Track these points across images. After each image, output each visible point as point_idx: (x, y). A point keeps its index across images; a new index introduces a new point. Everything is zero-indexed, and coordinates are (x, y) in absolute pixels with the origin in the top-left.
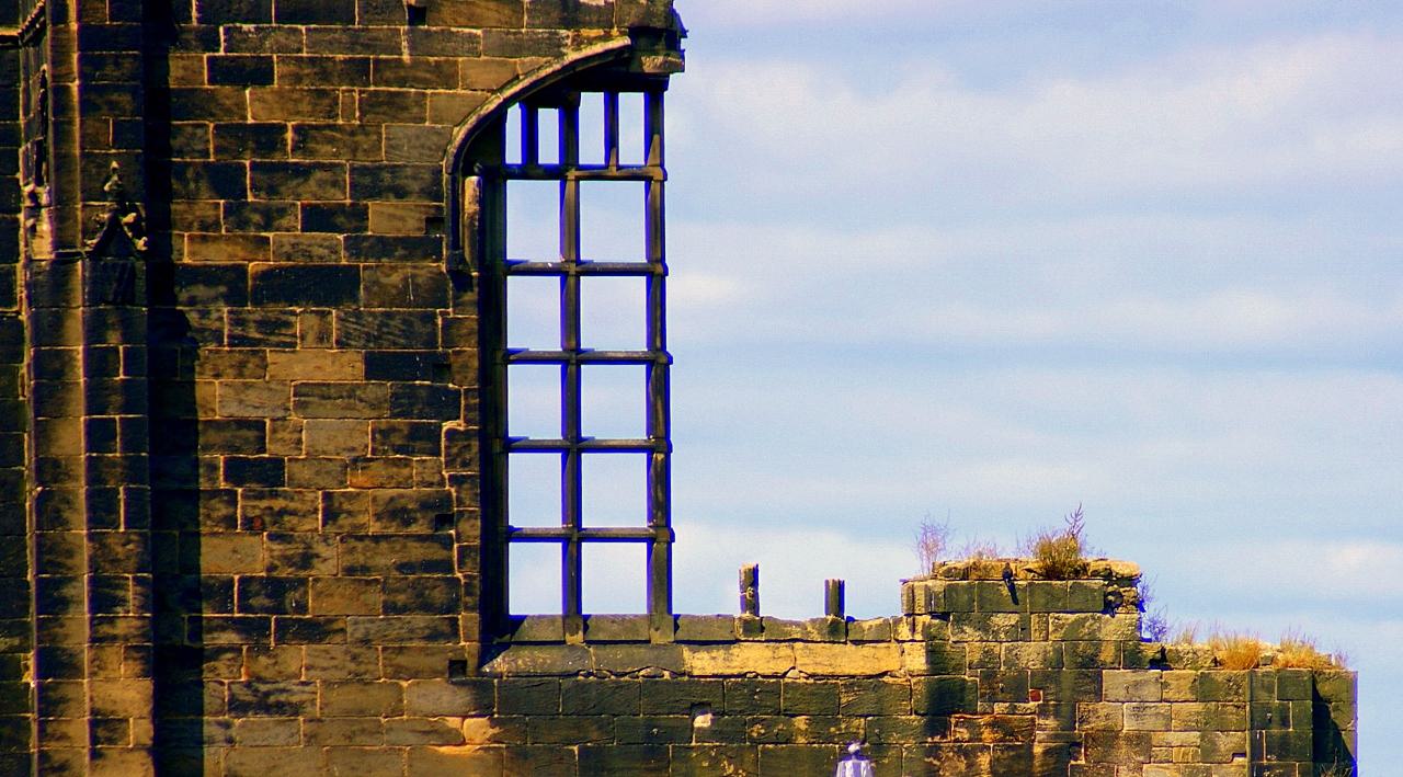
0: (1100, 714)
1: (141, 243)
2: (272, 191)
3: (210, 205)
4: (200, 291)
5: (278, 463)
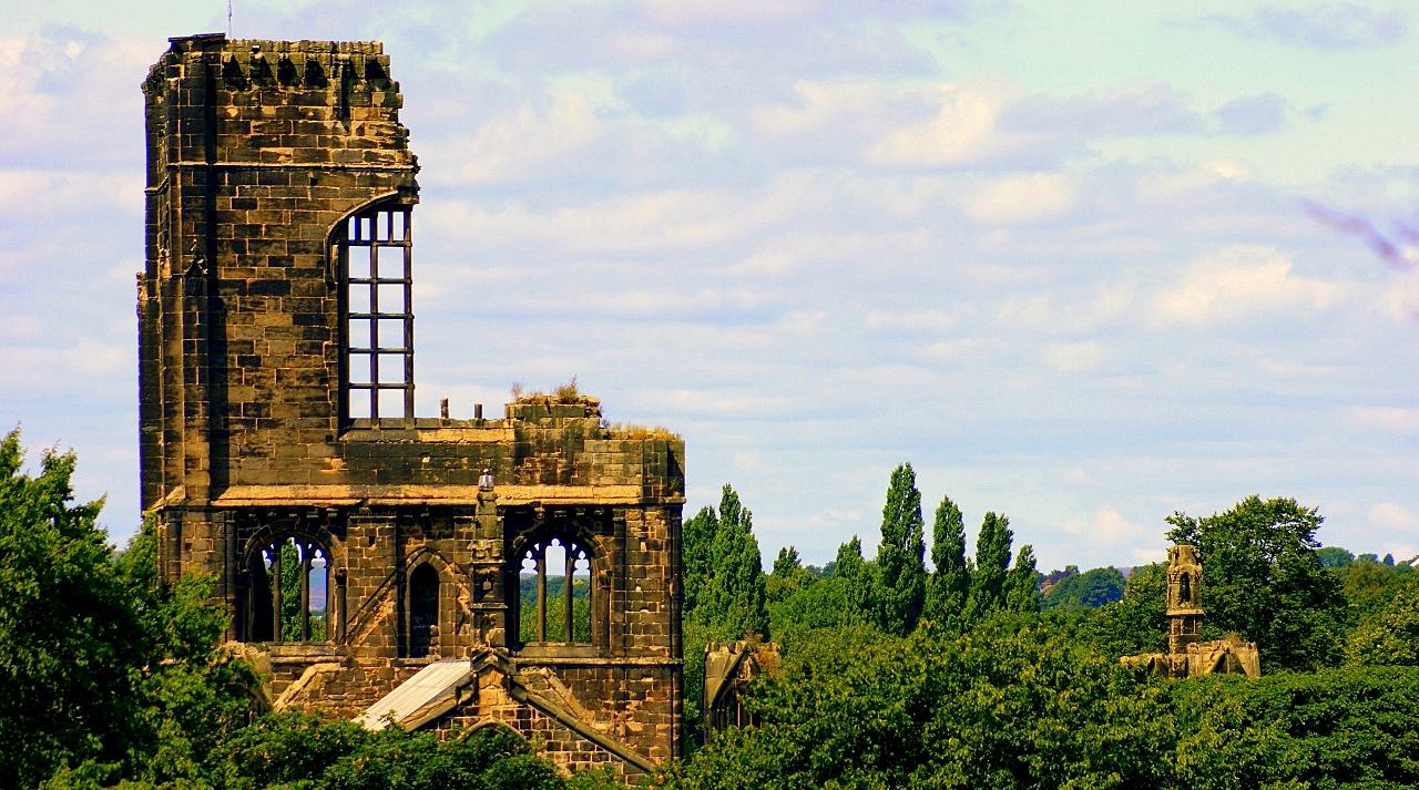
0: (583, 458)
3: (233, 257)
4: (228, 290)
5: (258, 358)
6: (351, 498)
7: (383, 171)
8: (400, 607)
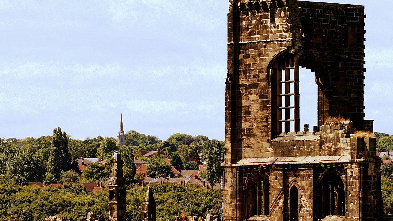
0: (340, 145)
1: (230, 82)
2: (249, 73)
3: (243, 76)
4: (242, 88)
5: (250, 112)
6: (270, 162)
7: (283, 41)
8: (285, 202)
